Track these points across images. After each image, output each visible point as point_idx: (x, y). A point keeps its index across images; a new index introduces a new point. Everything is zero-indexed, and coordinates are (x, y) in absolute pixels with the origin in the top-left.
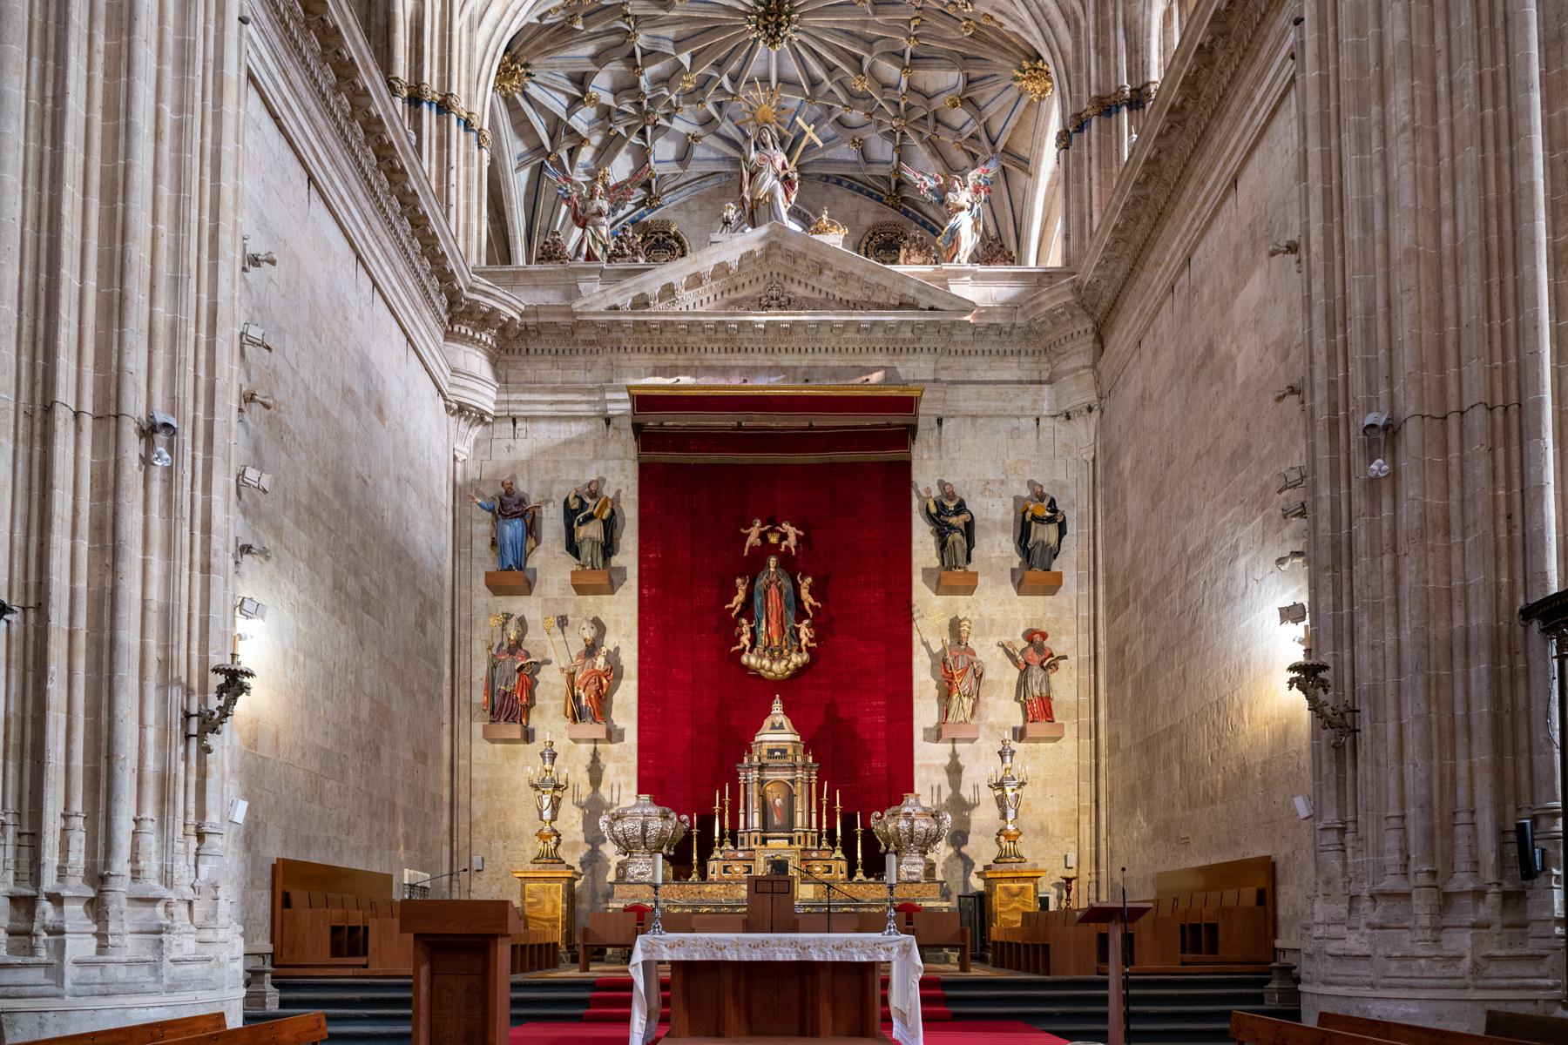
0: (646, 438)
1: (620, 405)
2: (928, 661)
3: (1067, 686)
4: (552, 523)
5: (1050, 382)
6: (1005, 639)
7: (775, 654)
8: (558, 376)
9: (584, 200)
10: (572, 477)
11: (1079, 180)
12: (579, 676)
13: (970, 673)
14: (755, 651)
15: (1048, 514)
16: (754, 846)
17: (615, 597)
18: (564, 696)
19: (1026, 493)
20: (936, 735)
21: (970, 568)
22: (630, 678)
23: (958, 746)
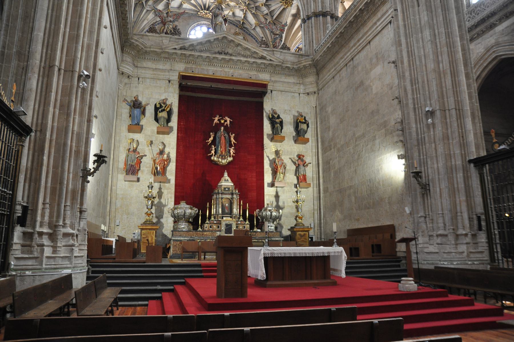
0: (182, 88)
1: (175, 77)
2: (269, 162)
3: (310, 172)
4: (150, 111)
5: (303, 84)
6: (292, 157)
7: (223, 157)
8: (154, 66)
9: (165, 17)
10: (157, 97)
11: (309, 32)
12: (157, 161)
13: (283, 166)
14: (216, 156)
15: (304, 121)
16: (220, 219)
17: (169, 136)
18: (152, 167)
19: (297, 114)
20: (272, 185)
21: (282, 134)
22: (173, 162)
23: (278, 189)
